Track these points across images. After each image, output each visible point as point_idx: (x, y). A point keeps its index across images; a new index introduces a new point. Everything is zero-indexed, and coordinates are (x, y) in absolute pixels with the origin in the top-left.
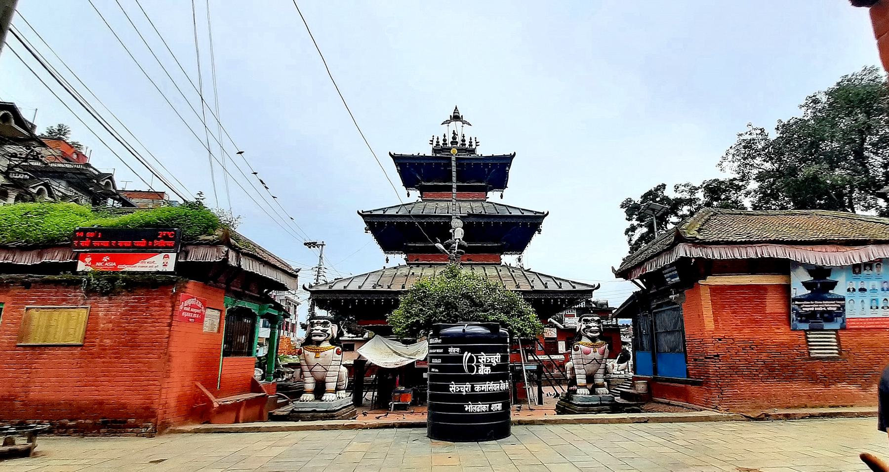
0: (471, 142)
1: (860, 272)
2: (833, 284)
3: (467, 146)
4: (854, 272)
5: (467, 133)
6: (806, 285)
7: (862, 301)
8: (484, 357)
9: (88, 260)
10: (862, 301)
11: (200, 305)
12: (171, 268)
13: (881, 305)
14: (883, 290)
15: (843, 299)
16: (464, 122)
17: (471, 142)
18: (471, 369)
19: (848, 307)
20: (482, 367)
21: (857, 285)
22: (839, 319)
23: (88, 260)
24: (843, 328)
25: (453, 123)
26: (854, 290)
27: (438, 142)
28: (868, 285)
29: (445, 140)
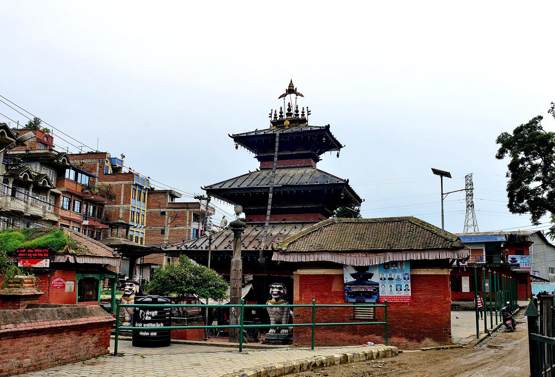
0: (303, 112)
1: (389, 268)
2: (371, 275)
3: (300, 117)
4: (385, 268)
5: (301, 103)
6: (353, 275)
7: (391, 286)
8: (148, 313)
9: (21, 262)
10: (391, 286)
11: (62, 280)
12: (48, 266)
13: (403, 288)
14: (405, 279)
15: (378, 284)
16: (298, 94)
17: (303, 112)
18: (142, 317)
19: (381, 289)
20: (147, 317)
21: (386, 276)
22: (376, 297)
23: (21, 262)
24: (378, 302)
25: (288, 96)
26: (385, 279)
27: (276, 115)
28: (394, 276)
29: (281, 113)
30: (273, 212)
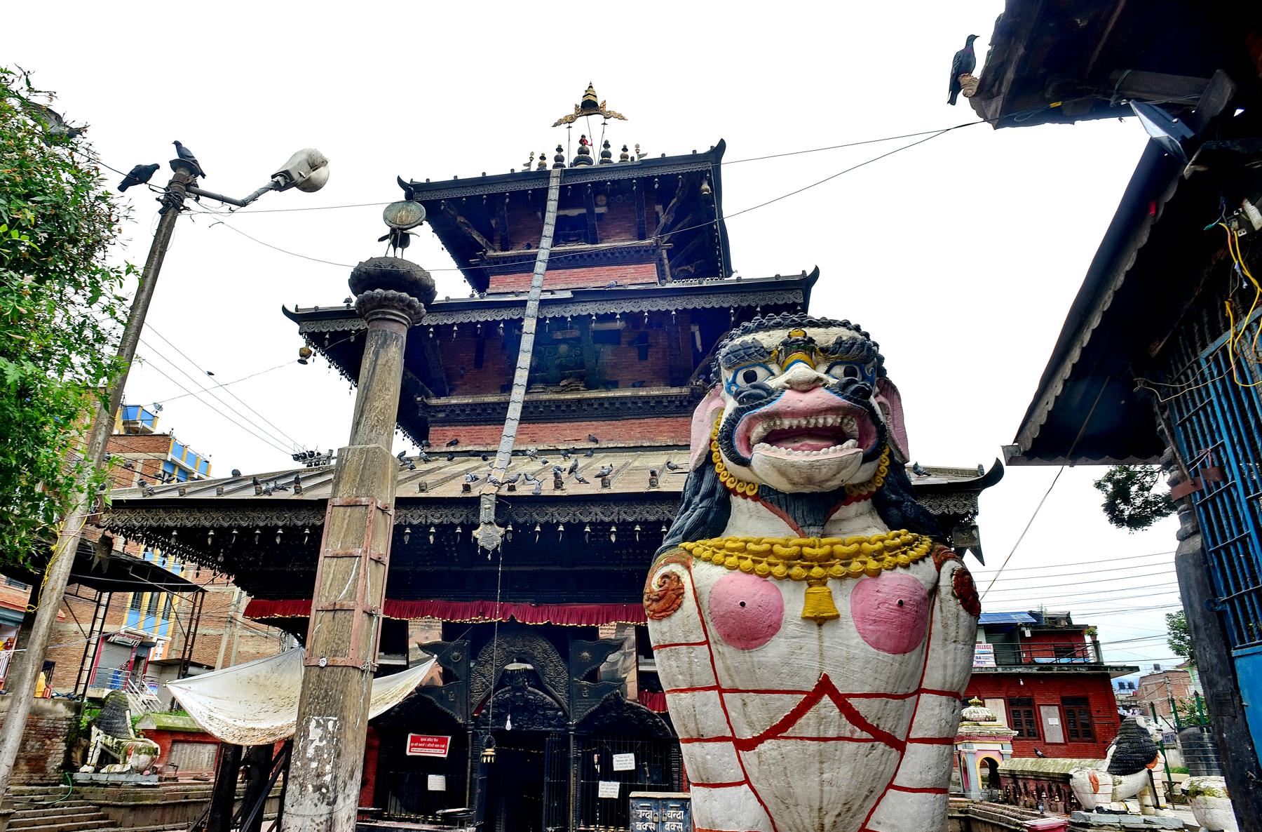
25: (582, 120)
30: (531, 414)
